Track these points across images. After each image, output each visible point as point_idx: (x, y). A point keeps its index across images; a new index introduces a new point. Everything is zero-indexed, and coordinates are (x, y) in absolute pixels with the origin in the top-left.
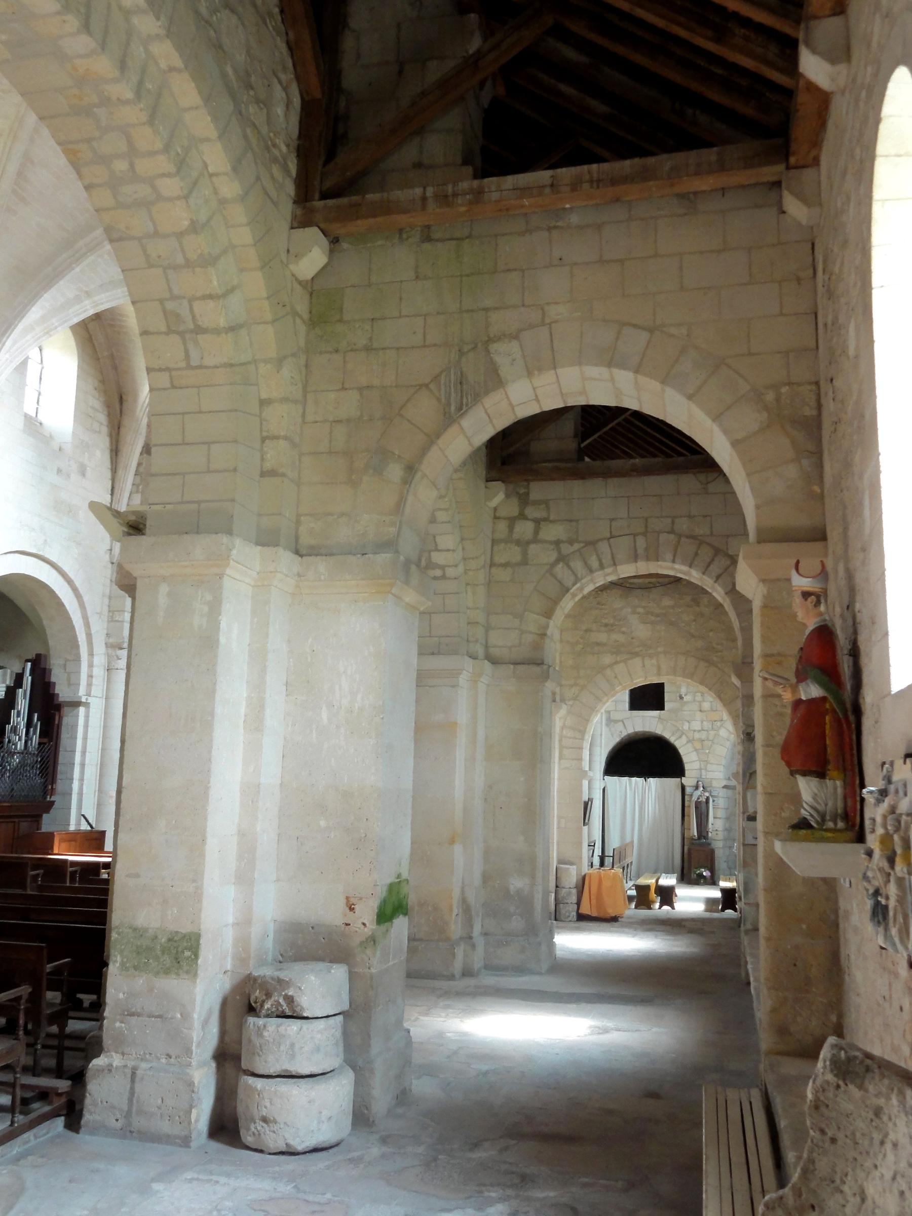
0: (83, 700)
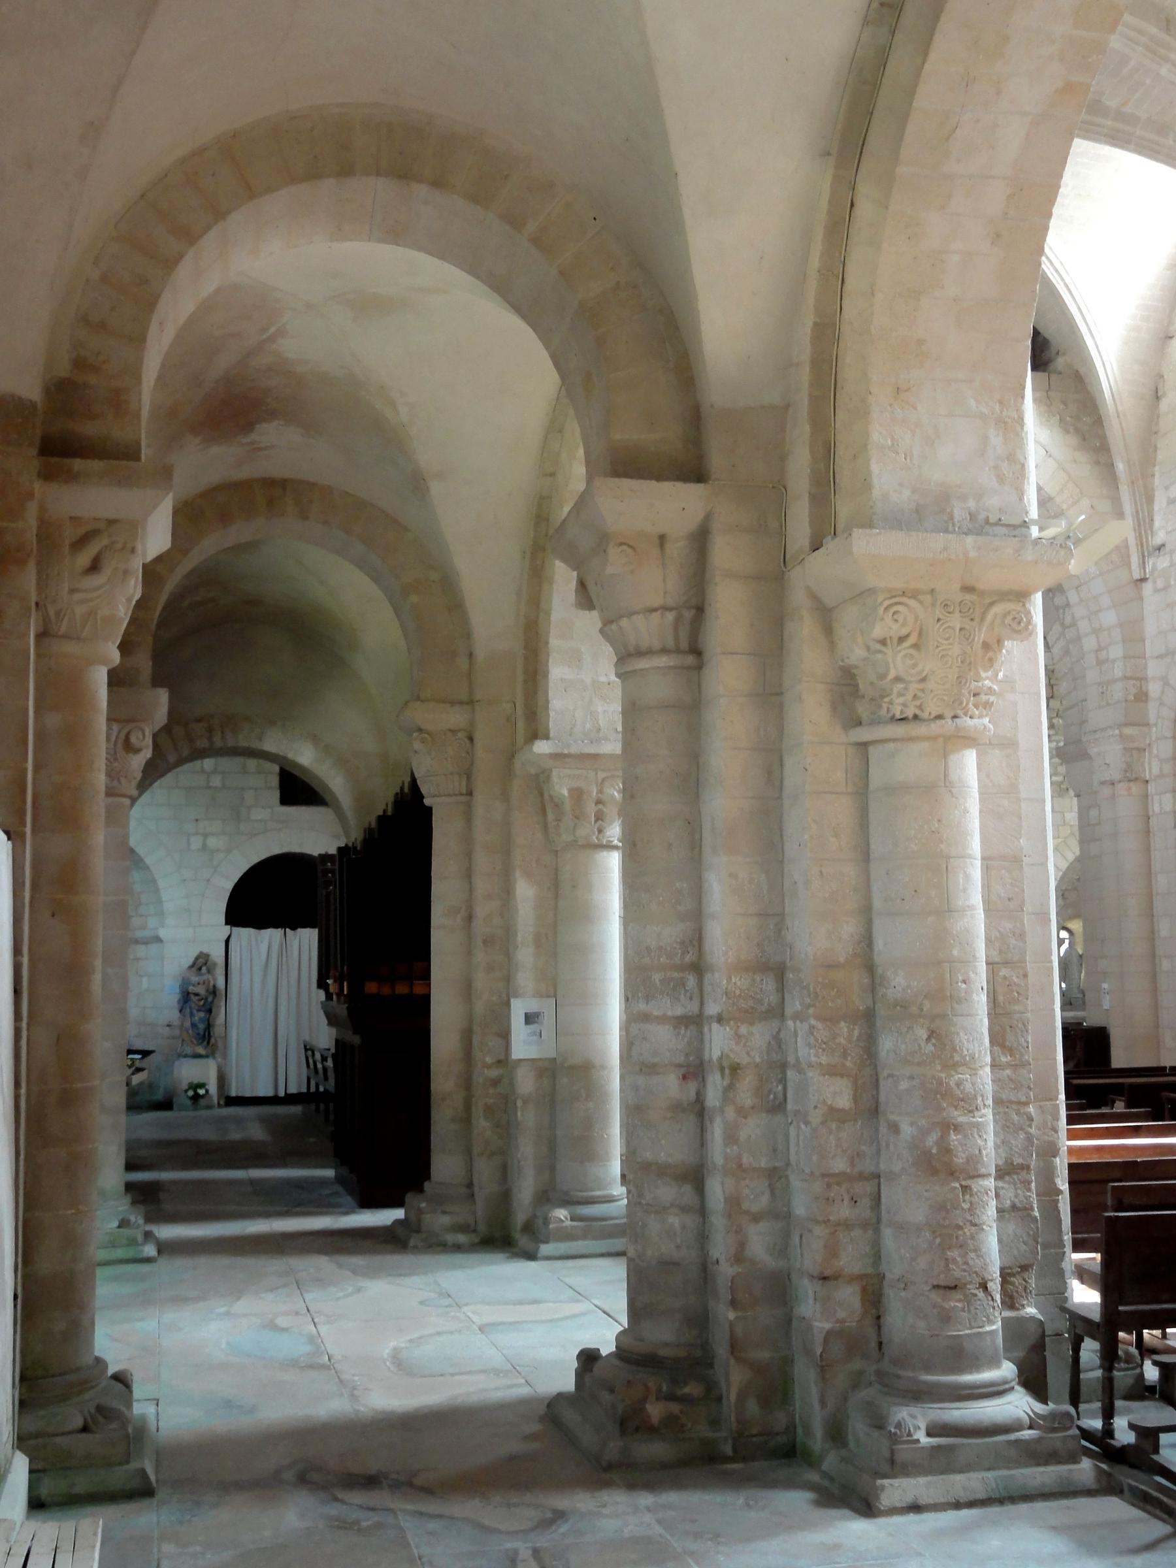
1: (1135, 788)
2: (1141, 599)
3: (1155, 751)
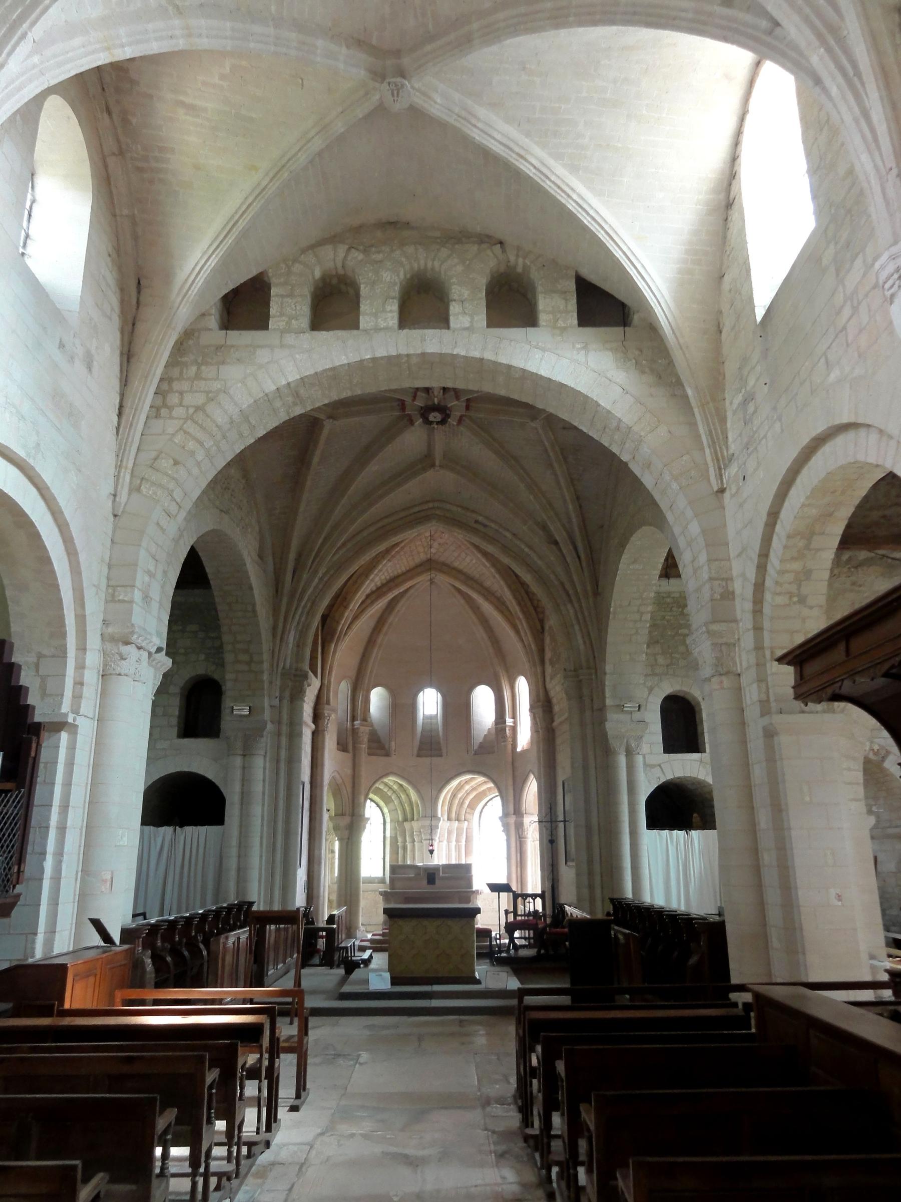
0: (70, 720)
1: (726, 682)
2: (723, 508)
3: (743, 645)
